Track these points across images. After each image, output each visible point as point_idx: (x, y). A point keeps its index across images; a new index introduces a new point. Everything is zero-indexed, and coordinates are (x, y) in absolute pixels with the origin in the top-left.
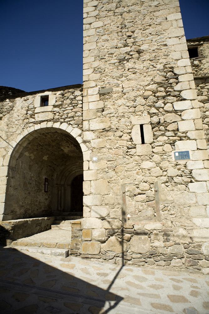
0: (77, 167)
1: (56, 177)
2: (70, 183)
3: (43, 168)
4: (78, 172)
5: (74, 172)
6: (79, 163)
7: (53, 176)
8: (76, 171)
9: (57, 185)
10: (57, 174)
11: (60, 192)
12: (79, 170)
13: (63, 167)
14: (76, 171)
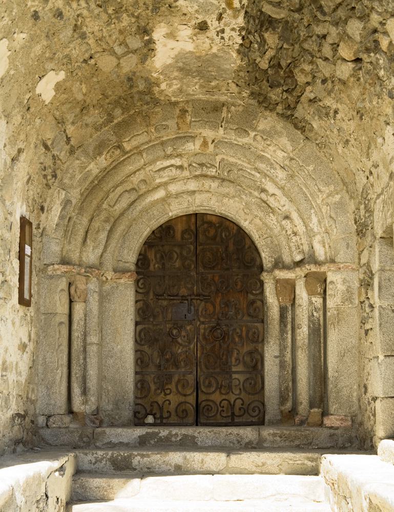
0: (181, 167)
1: (61, 217)
2: (131, 258)
3: (20, 151)
4: (178, 195)
5: (160, 194)
6: (205, 144)
7: (42, 209)
8: (173, 188)
9: (64, 268)
10: (67, 203)
11: (79, 308)
12: (192, 185)
13: (103, 161)
14: (173, 188)
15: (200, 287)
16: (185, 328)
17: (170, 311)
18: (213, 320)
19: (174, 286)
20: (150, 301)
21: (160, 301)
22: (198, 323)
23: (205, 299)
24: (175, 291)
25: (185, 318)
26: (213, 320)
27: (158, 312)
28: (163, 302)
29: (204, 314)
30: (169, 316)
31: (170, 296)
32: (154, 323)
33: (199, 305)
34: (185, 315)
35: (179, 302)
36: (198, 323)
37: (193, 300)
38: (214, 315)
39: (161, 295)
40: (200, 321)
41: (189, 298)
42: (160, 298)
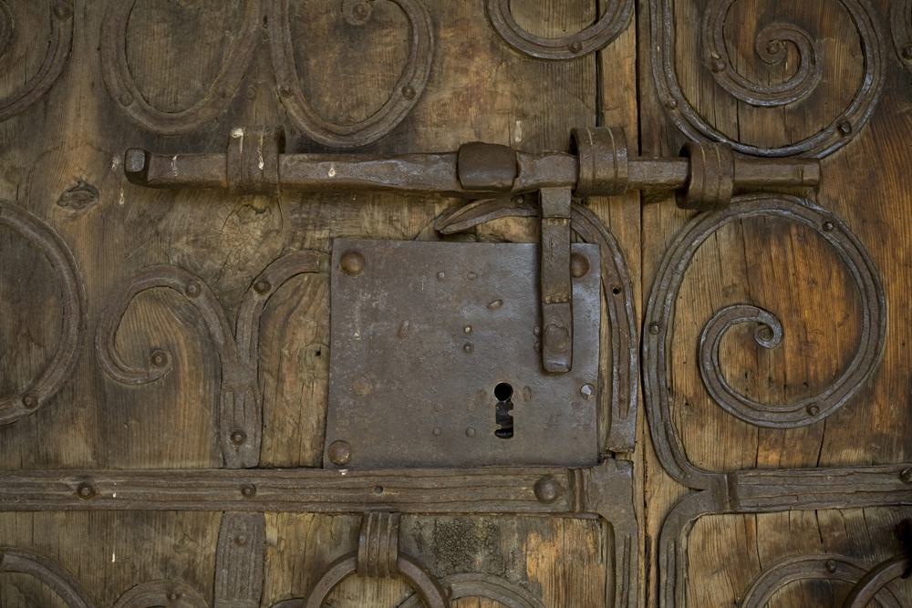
15: (685, 41)
16: (501, 564)
17: (304, 335)
18: (852, 455)
19: (351, 32)
20: (58, 215)
21: (182, 215)
22: (663, 491)
23: (741, 190)
24: (369, 93)
25: (506, 430)
26: (852, 455)
27: (154, 356)
28: (222, 221)
29: (730, 372)
30: (301, 401)
31: (310, 147)
32: (111, 490)
33: (667, 264)
34: (504, 391)
35: (413, 220)
36: (663, 491)
37: (599, 210)
38: (868, 395)
39: (193, 144)
40: (674, 457)
41: (552, 172)
42: (176, 169)
